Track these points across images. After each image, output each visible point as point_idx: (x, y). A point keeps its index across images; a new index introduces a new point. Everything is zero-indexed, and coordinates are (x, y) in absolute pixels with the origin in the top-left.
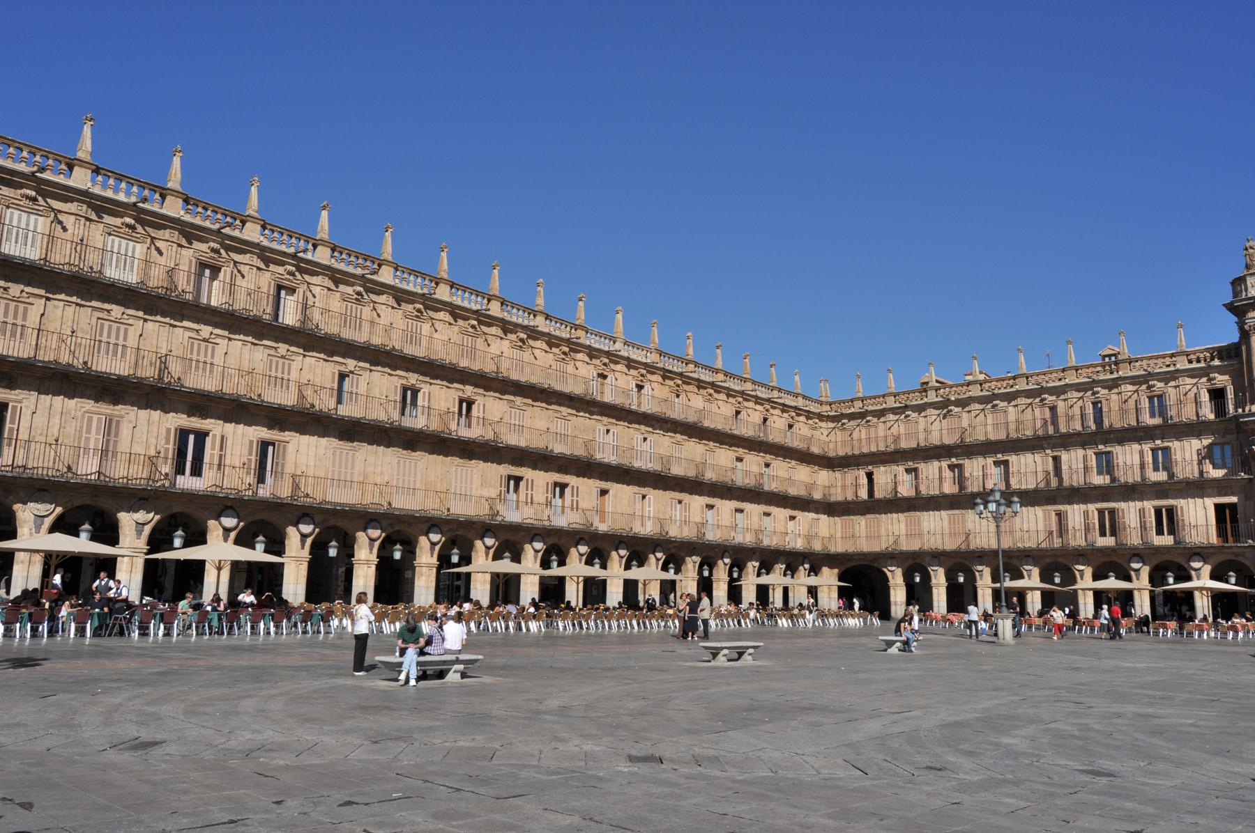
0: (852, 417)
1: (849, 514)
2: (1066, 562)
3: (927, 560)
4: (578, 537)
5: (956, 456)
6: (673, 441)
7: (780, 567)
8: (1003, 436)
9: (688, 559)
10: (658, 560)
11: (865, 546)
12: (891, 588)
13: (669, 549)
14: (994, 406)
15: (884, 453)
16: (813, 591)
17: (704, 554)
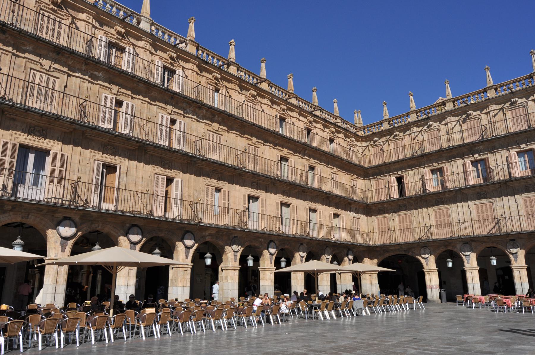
0: (382, 134)
3: (459, 246)
4: (60, 216)
5: (479, 152)
7: (327, 257)
9: (228, 249)
10: (188, 248)
11: (401, 238)
12: (426, 274)
13: (203, 237)
14: (512, 104)
15: (412, 158)
16: (356, 277)
17: (247, 244)
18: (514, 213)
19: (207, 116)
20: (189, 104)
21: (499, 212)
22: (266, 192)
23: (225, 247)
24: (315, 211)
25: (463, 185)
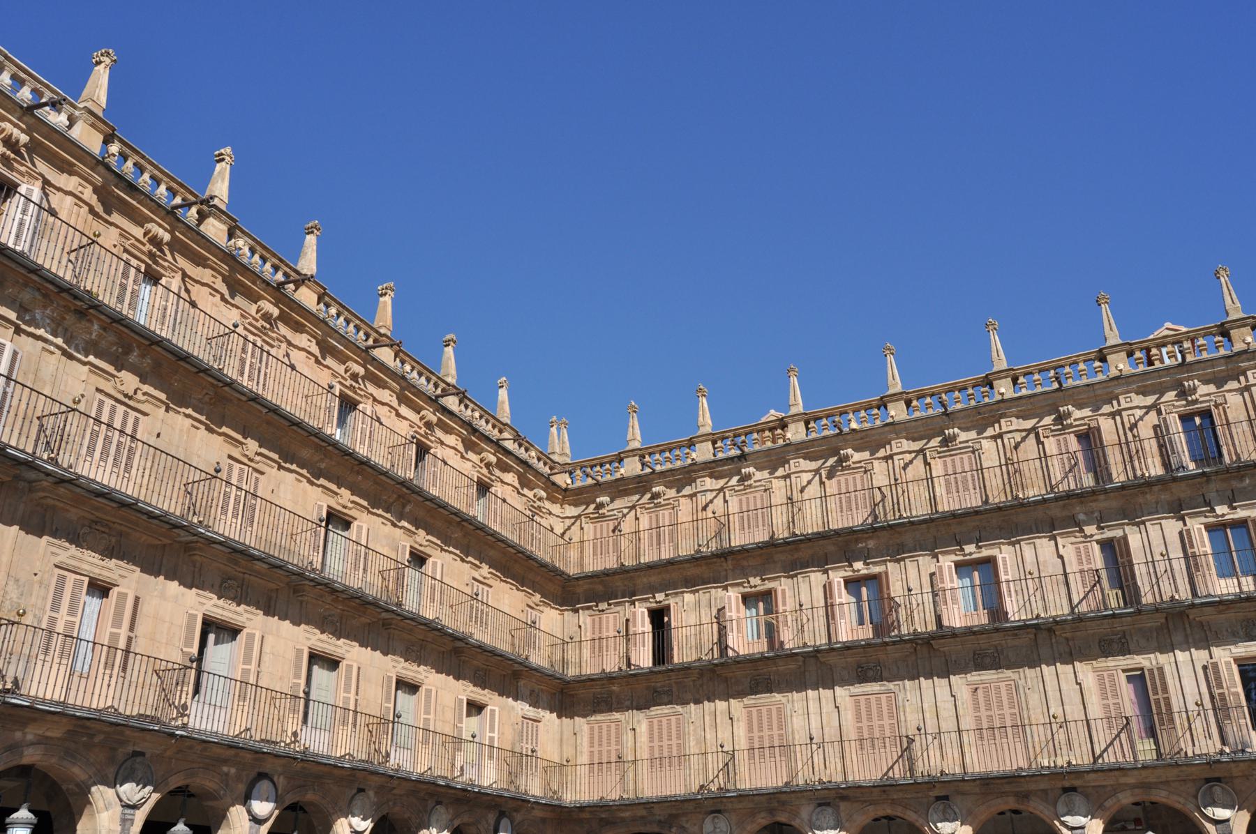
0: (620, 488)
1: (610, 709)
2: (1177, 802)
3: (805, 812)
5: (866, 557)
6: (108, 386)
8: (973, 500)
9: (102, 795)
14: (946, 441)
15: (696, 559)
17: (175, 782)
18: (948, 724)
19: (103, 344)
20: (45, 296)
21: (911, 721)
22: (267, 613)
23: (94, 789)
24: (412, 688)
25: (821, 640)
